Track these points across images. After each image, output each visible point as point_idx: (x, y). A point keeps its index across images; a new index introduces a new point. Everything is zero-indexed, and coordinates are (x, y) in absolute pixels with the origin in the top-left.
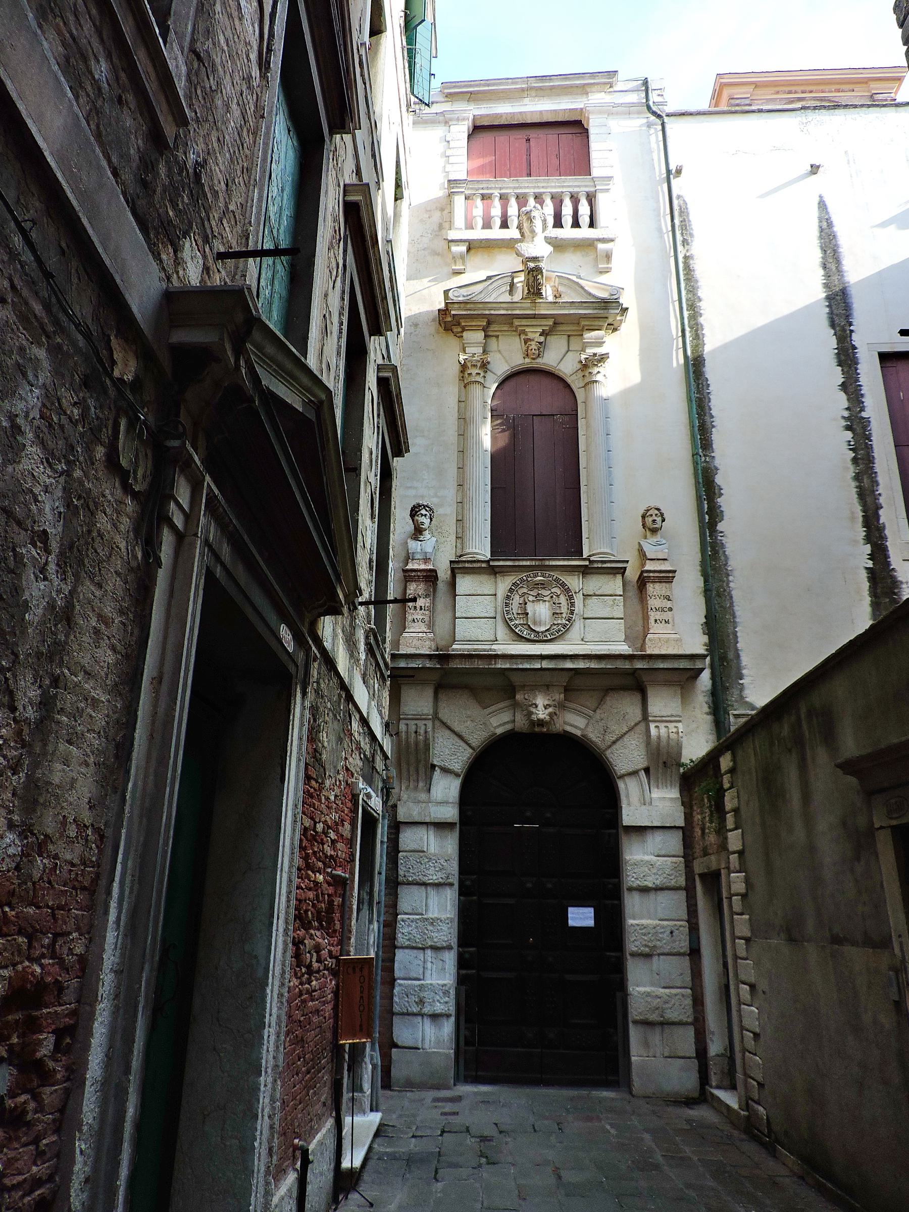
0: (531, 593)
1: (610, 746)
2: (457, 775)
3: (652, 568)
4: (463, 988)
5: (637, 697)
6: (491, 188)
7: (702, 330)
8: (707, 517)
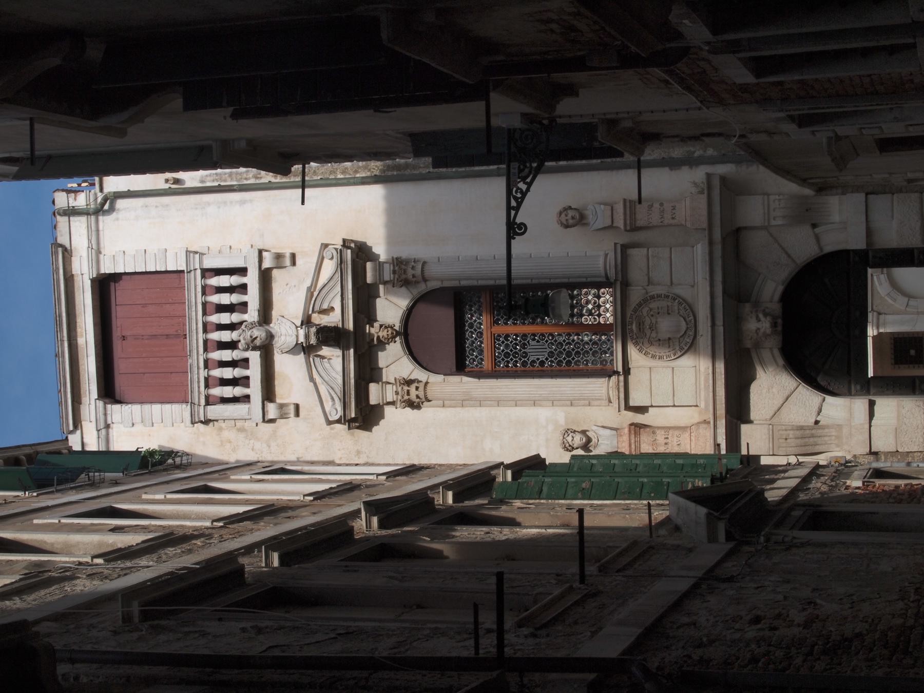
0: (648, 335)
1: (793, 261)
6: (198, 378)
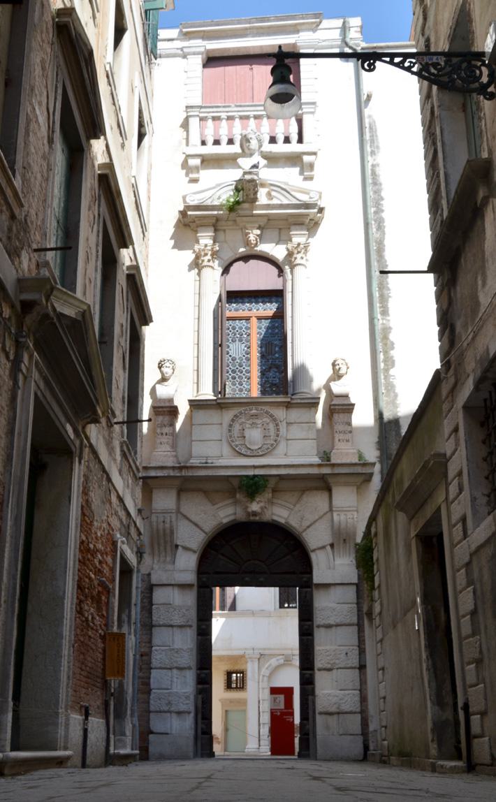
0: (248, 422)
1: (305, 530)
2: (195, 552)
3: (337, 403)
4: (200, 696)
5: (325, 495)
7: (384, 222)
8: (382, 365)
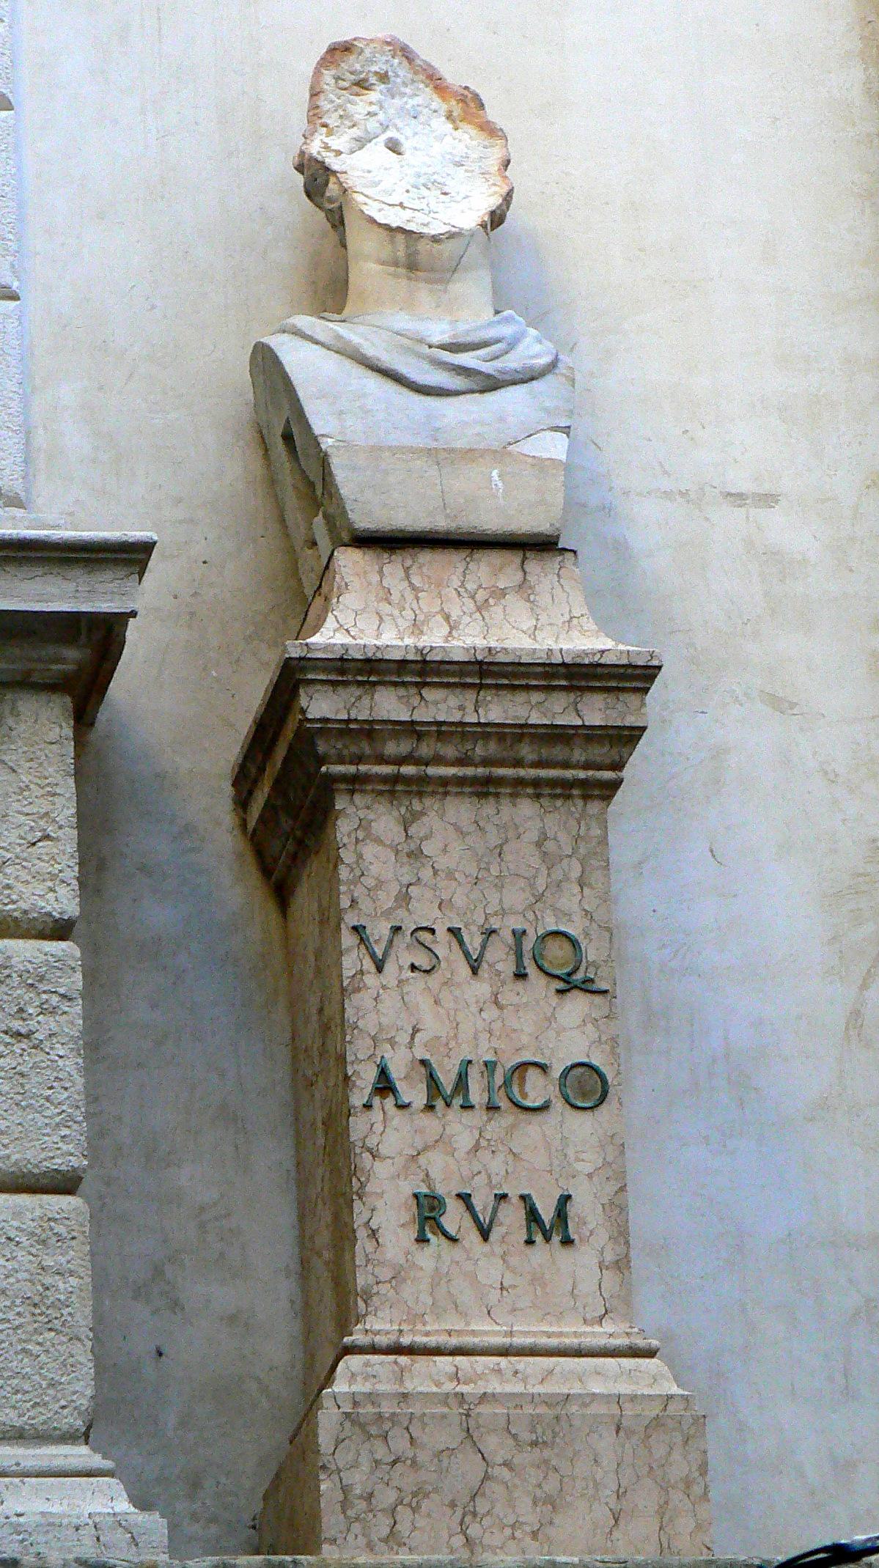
3: (392, 638)
